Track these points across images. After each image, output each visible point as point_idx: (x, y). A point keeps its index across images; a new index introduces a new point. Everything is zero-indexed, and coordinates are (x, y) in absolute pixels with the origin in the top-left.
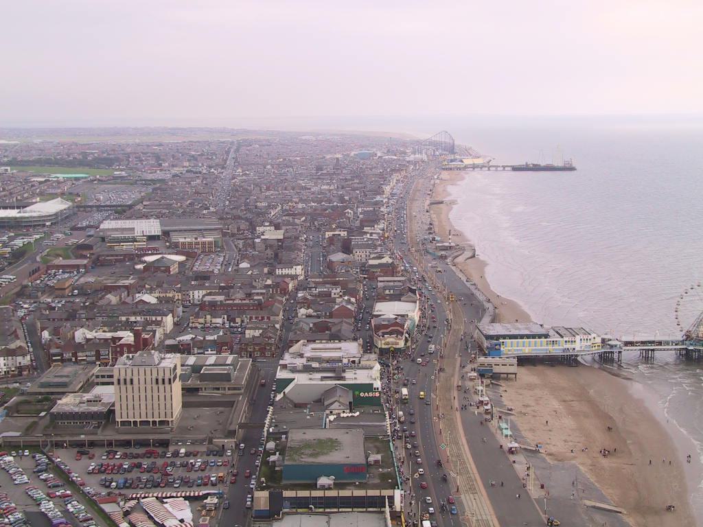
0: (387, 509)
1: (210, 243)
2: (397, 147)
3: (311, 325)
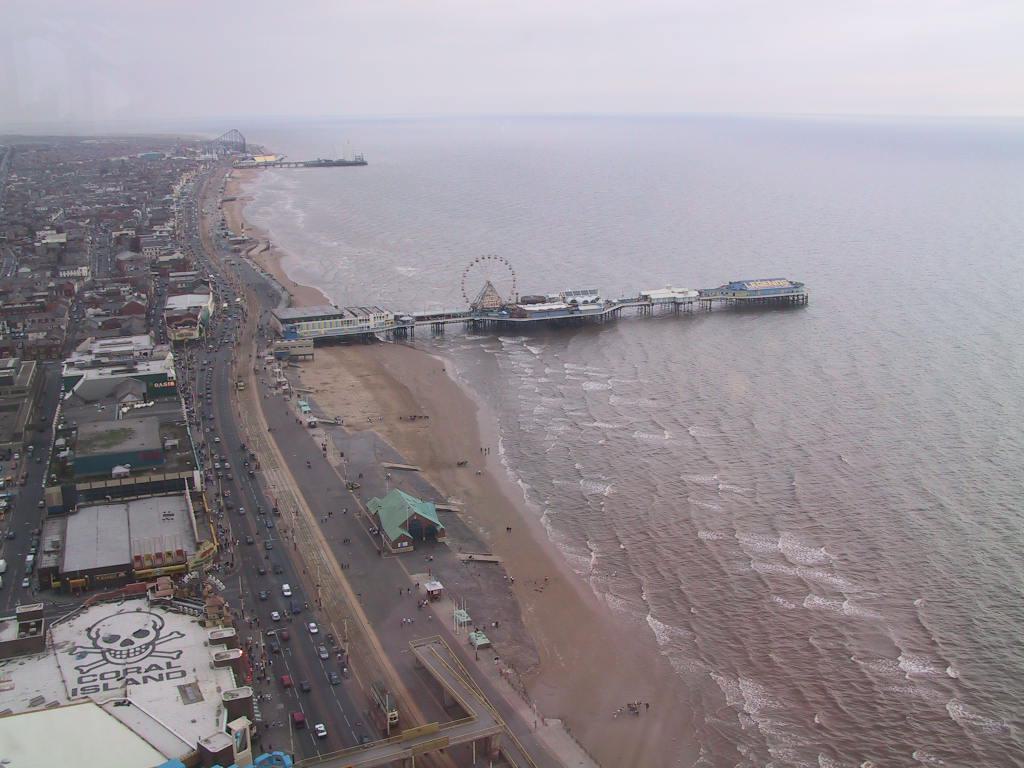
0: (188, 491)
2: (185, 147)
3: (100, 324)
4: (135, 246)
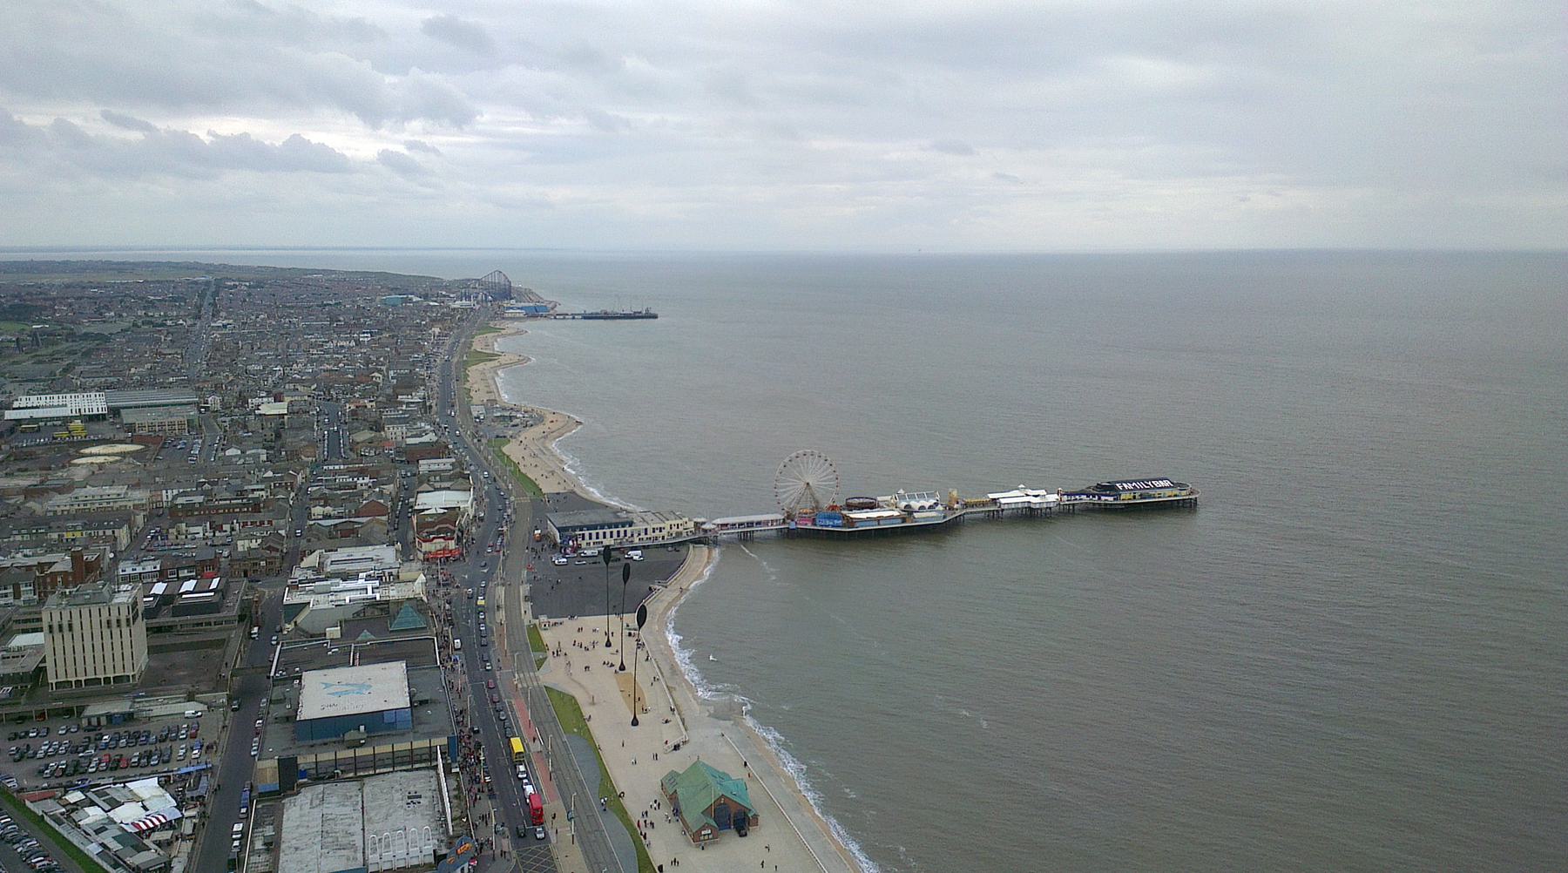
1: (180, 424)
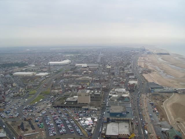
0: (130, 122)
1: (96, 68)
4: (123, 70)
